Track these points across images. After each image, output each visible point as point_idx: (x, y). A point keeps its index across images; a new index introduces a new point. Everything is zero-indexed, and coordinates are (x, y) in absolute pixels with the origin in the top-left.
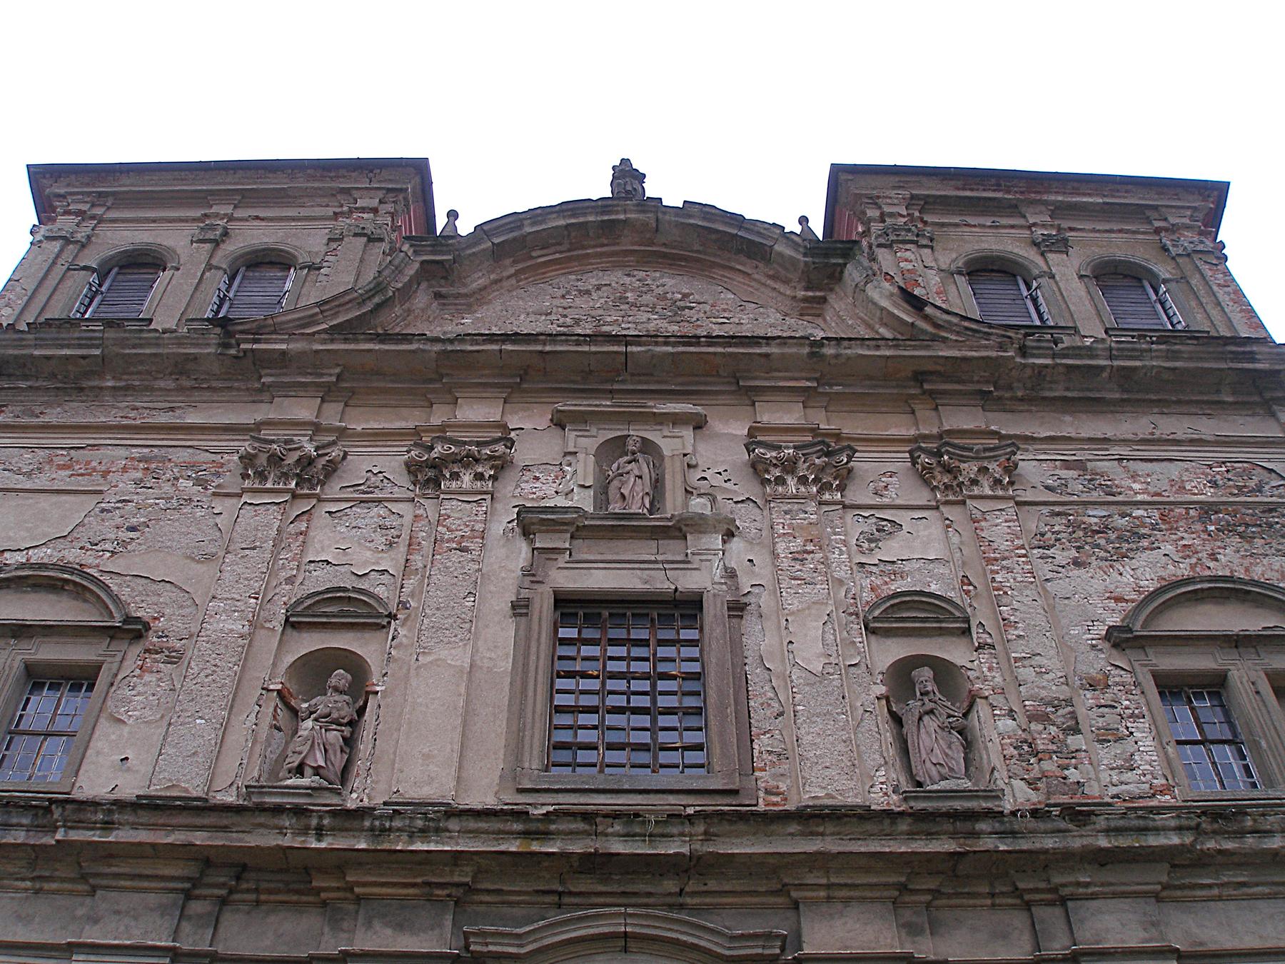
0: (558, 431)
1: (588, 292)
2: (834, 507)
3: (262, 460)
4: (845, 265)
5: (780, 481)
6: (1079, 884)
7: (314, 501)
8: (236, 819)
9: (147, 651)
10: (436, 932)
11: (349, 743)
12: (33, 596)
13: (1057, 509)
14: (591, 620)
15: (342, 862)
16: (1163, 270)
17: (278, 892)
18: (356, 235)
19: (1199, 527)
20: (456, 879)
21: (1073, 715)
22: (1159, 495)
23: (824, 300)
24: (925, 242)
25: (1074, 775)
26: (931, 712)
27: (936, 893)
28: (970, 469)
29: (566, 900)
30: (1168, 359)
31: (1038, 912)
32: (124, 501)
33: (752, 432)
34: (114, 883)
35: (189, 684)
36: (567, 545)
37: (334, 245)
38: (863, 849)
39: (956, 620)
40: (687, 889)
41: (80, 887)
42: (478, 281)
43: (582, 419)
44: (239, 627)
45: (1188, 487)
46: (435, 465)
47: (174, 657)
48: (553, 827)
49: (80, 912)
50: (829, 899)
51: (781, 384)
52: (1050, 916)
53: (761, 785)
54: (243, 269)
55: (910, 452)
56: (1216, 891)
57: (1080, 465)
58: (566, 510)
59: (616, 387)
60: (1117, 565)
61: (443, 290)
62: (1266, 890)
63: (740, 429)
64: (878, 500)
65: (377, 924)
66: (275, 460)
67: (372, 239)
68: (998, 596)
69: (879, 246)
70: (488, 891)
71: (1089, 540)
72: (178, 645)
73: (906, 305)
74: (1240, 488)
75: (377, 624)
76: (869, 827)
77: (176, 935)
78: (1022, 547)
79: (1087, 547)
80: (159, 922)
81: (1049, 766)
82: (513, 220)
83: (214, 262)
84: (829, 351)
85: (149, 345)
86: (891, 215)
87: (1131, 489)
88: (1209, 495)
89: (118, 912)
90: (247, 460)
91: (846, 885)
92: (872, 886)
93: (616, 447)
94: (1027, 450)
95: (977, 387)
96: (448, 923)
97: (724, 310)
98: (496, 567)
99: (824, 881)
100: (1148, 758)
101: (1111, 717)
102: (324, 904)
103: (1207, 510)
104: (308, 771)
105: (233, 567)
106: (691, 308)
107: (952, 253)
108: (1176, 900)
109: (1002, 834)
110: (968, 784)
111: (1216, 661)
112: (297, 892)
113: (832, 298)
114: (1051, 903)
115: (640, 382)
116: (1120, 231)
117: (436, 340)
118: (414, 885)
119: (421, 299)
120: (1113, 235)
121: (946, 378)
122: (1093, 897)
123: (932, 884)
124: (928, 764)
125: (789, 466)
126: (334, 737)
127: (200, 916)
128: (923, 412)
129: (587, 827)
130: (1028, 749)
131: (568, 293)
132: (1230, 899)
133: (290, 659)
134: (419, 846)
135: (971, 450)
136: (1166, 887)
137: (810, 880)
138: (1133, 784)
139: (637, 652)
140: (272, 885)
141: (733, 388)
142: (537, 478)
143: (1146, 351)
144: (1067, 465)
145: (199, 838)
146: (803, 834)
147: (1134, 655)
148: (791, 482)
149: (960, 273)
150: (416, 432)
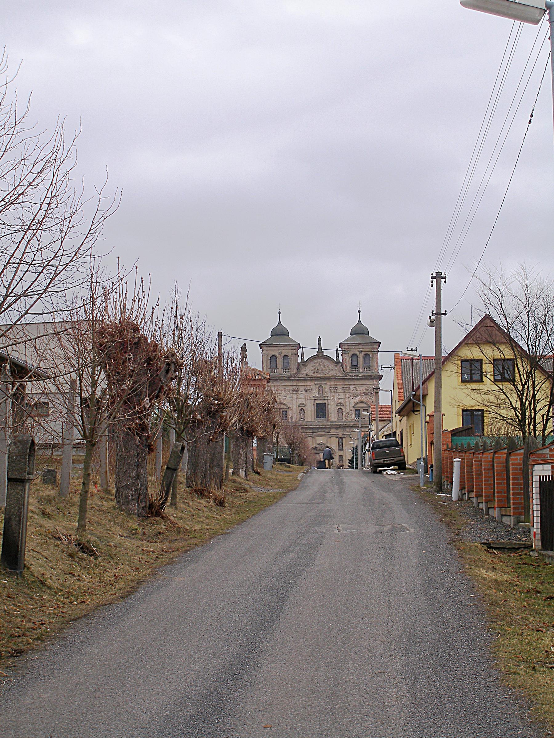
46: (307, 390)
66: (294, 390)
93: (320, 386)
107: (350, 354)
119: (302, 367)
138: (352, 419)
150: (304, 385)
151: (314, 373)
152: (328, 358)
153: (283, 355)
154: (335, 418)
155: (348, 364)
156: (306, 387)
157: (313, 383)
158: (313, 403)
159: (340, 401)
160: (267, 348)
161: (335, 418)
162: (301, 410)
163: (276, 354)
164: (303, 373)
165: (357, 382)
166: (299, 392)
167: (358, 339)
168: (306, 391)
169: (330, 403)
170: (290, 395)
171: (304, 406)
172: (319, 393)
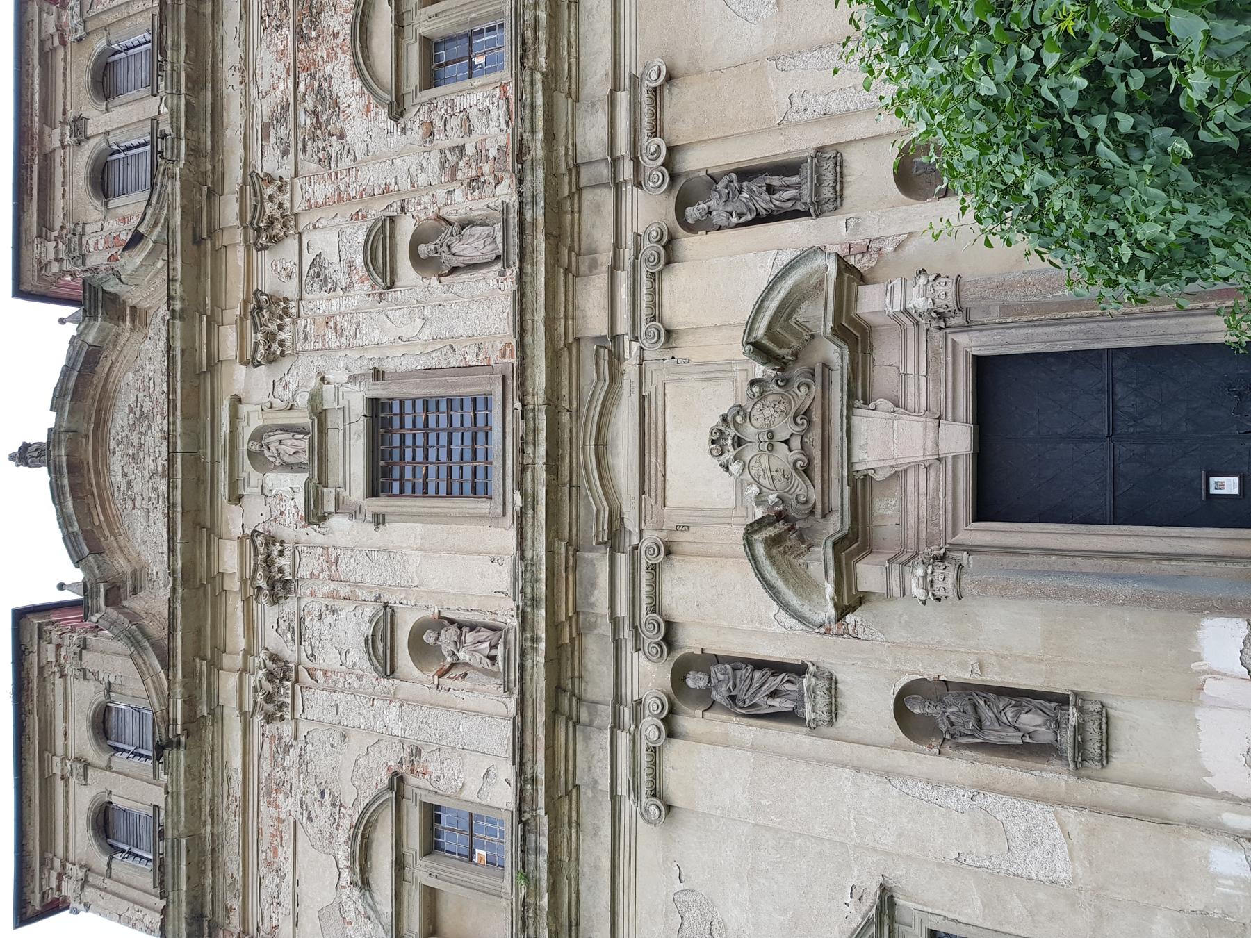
0: (244, 500)
1: (129, 483)
2: (301, 307)
3: (270, 707)
4: (104, 291)
5: (282, 344)
6: (566, 154)
7: (300, 667)
8: (528, 695)
9: (412, 771)
10: (596, 562)
11: (473, 627)
12: (374, 859)
13: (300, 146)
14: (386, 473)
15: (554, 626)
16: (99, 44)
17: (573, 664)
18: (80, 659)
19: (313, 44)
20: (563, 551)
21: (452, 149)
22: (288, 70)
23: (133, 308)
24: (79, 229)
25: (493, 153)
26: (449, 246)
27: (571, 249)
28: (270, 208)
29: (574, 483)
30: (178, 51)
31: (583, 183)
32: (302, 805)
33: (245, 363)
34: (571, 772)
35: (435, 739)
36: (333, 490)
37: (89, 675)
38: (543, 295)
39: (384, 225)
40: (567, 407)
41: (574, 796)
42: (120, 564)
43: (234, 483)
44: (394, 709)
45: (282, 48)
46: (272, 584)
47: (417, 752)
48: (530, 491)
49: (590, 794)
50: (574, 318)
51: (205, 341)
52: (585, 176)
53: (500, 360)
54: (109, 742)
55: (258, 250)
56: (573, 61)
57: (266, 127)
58: (307, 492)
59: (209, 460)
60: (343, 107)
61: (129, 588)
62: (573, 25)
63: (241, 371)
64: (295, 276)
65: (592, 600)
66: (269, 698)
67: (84, 645)
68: (365, 195)
69: (84, 264)
70: (570, 530)
71: (323, 127)
72: (406, 752)
73: (139, 246)
74: (283, 8)
75: (391, 616)
76: (528, 291)
77: (601, 729)
78: (330, 175)
79: (329, 128)
80: (595, 740)
81: (487, 169)
82: (70, 540)
83: (104, 764)
84: (178, 305)
85: (178, 804)
86: (56, 253)
87: (284, 92)
88: (288, 33)
89: (590, 767)
90: (269, 718)
91: (565, 307)
92: (566, 291)
94: (254, 166)
95: (205, 197)
96: (589, 555)
97: (143, 382)
98: (349, 538)
99: (563, 321)
100: (481, 100)
101: (453, 122)
102: (579, 635)
103: (300, 36)
104: (493, 652)
105: (351, 719)
106: (142, 406)
107: (91, 210)
108: (578, 88)
109: (534, 203)
110: (498, 227)
111: (413, 43)
112: (573, 653)
113: (131, 302)
114: (578, 174)
115: (205, 442)
116: (65, 74)
117: (174, 590)
118: (567, 578)
120: (69, 80)
121: (198, 220)
122: (574, 145)
123: (565, 252)
124: (484, 251)
125: (270, 337)
126: (470, 637)
127: (590, 714)
128: (225, 239)
129: (530, 470)
130: (475, 182)
131: (130, 497)
132: (578, 51)
133: (416, 673)
134: (543, 576)
135: (255, 207)
136: (569, 95)
137: (562, 330)
138: (499, 112)
139: (409, 442)
140: (569, 668)
141: (209, 376)
142: (282, 513)
143: (172, 67)
144: (265, 136)
145: (541, 718)
146: (533, 334)
147: (408, 103)
148: (281, 336)
149: (106, 204)
150: (246, 600)
157: (235, 520)
158: (363, 532)
159: (359, 261)
165: (234, 117)
168: (279, 588)
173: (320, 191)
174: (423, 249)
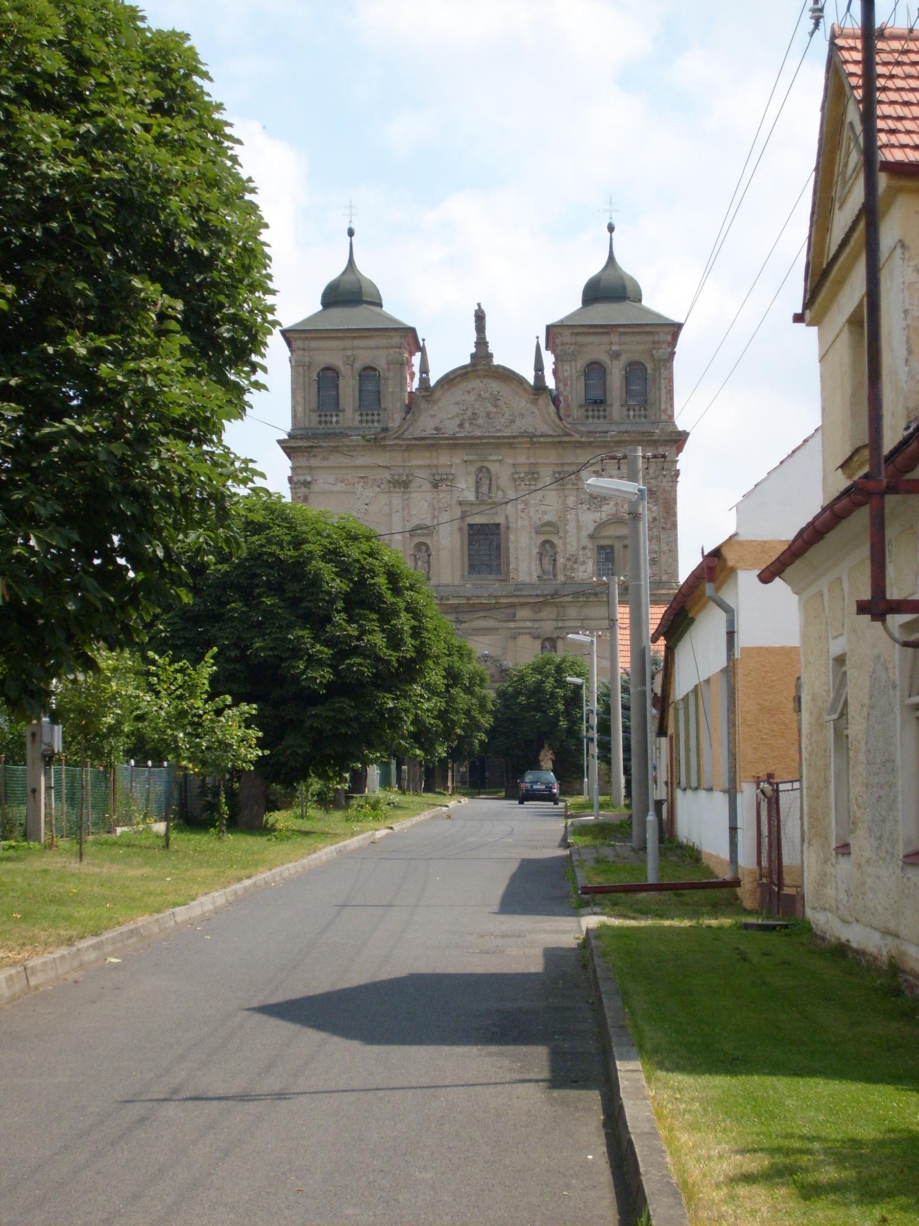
16: (649, 366)
25: (573, 575)
42: (438, 394)
43: (471, 462)
63: (510, 461)
84: (535, 440)
93: (480, 470)
107: (581, 364)
119: (423, 405)
125: (522, 479)
126: (426, 565)
133: (413, 545)
138: (585, 576)
151: (461, 425)
152: (507, 376)
153: (358, 365)
154: (530, 574)
155: (576, 394)
156: (434, 471)
157: (457, 458)
159: (546, 518)
160: (307, 344)
161: (530, 574)
162: (419, 546)
163: (337, 361)
164: (425, 424)
166: (414, 486)
167: (604, 314)
169: (511, 525)
170: (383, 499)
171: (430, 535)
172: (477, 492)
173: (571, 501)
174: (547, 546)
